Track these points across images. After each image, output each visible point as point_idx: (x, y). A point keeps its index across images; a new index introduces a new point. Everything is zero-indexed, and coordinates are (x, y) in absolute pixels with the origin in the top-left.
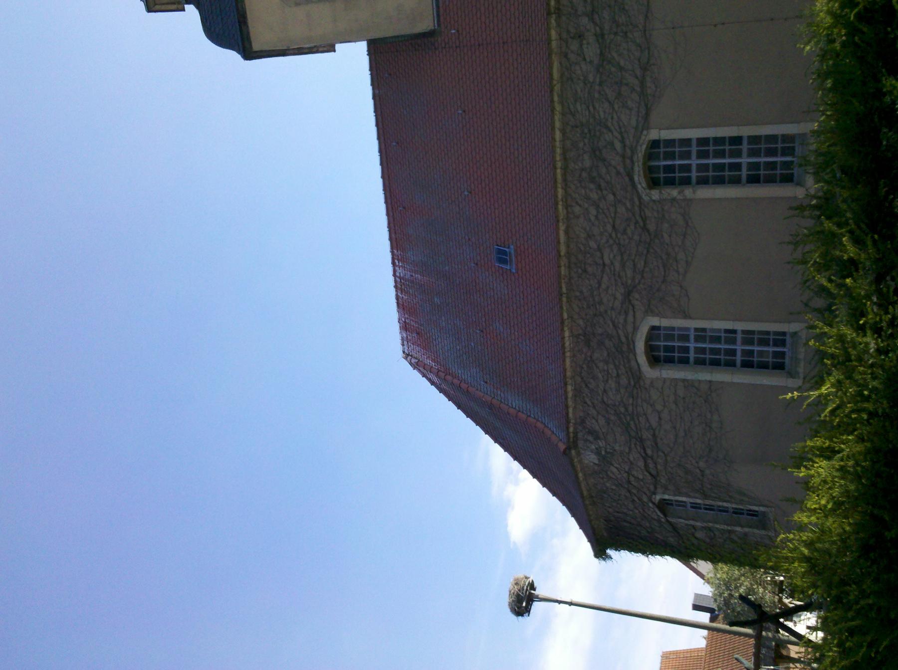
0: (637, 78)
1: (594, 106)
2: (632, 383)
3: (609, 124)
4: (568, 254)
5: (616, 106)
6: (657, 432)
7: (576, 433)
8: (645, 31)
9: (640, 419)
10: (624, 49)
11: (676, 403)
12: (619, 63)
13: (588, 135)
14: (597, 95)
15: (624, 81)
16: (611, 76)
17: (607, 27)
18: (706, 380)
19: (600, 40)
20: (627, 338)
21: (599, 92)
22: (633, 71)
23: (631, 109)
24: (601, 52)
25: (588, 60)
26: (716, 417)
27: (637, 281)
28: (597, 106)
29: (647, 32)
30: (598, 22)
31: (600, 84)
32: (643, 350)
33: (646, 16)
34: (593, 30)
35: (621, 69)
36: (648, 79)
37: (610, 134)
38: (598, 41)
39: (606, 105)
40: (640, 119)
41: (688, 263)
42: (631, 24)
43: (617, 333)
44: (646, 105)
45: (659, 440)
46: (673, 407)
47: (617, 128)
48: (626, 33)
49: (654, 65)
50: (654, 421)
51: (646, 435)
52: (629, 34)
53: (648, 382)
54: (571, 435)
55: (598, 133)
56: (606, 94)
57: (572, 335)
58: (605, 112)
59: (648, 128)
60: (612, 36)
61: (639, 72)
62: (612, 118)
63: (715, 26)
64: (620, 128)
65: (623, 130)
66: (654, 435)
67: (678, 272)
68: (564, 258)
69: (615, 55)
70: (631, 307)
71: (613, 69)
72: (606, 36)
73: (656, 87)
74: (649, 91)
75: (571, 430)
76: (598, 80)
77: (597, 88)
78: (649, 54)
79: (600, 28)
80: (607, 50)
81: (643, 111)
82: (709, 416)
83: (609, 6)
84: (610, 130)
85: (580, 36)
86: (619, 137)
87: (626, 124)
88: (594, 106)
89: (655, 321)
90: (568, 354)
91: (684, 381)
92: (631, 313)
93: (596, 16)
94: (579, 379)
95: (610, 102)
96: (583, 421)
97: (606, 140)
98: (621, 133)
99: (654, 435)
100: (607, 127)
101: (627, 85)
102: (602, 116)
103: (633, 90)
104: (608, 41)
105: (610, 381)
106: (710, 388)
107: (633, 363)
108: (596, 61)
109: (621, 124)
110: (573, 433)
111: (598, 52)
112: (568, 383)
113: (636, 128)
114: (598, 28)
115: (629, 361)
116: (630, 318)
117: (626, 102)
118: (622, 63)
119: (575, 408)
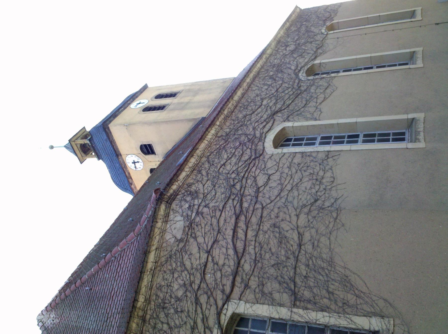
2: (253, 157)
4: (239, 102)
6: (261, 189)
7: (176, 194)
9: (249, 181)
11: (289, 168)
18: (324, 151)
20: (261, 134)
26: (329, 174)
27: (283, 109)
32: (272, 139)
41: (325, 99)
43: (255, 133)
45: (260, 195)
46: (286, 171)
50: (261, 180)
51: (249, 191)
53: (267, 157)
54: (171, 191)
57: (216, 135)
66: (258, 191)
67: (317, 102)
68: (234, 102)
70: (272, 120)
75: (174, 187)
82: (321, 173)
89: (289, 124)
90: (206, 142)
91: (302, 153)
92: (272, 122)
94: (204, 159)
96: (190, 185)
99: (258, 191)
105: (232, 159)
106: (327, 156)
107: (260, 147)
110: (174, 191)
112: (194, 157)
115: (257, 145)
116: (270, 124)
119: (188, 176)
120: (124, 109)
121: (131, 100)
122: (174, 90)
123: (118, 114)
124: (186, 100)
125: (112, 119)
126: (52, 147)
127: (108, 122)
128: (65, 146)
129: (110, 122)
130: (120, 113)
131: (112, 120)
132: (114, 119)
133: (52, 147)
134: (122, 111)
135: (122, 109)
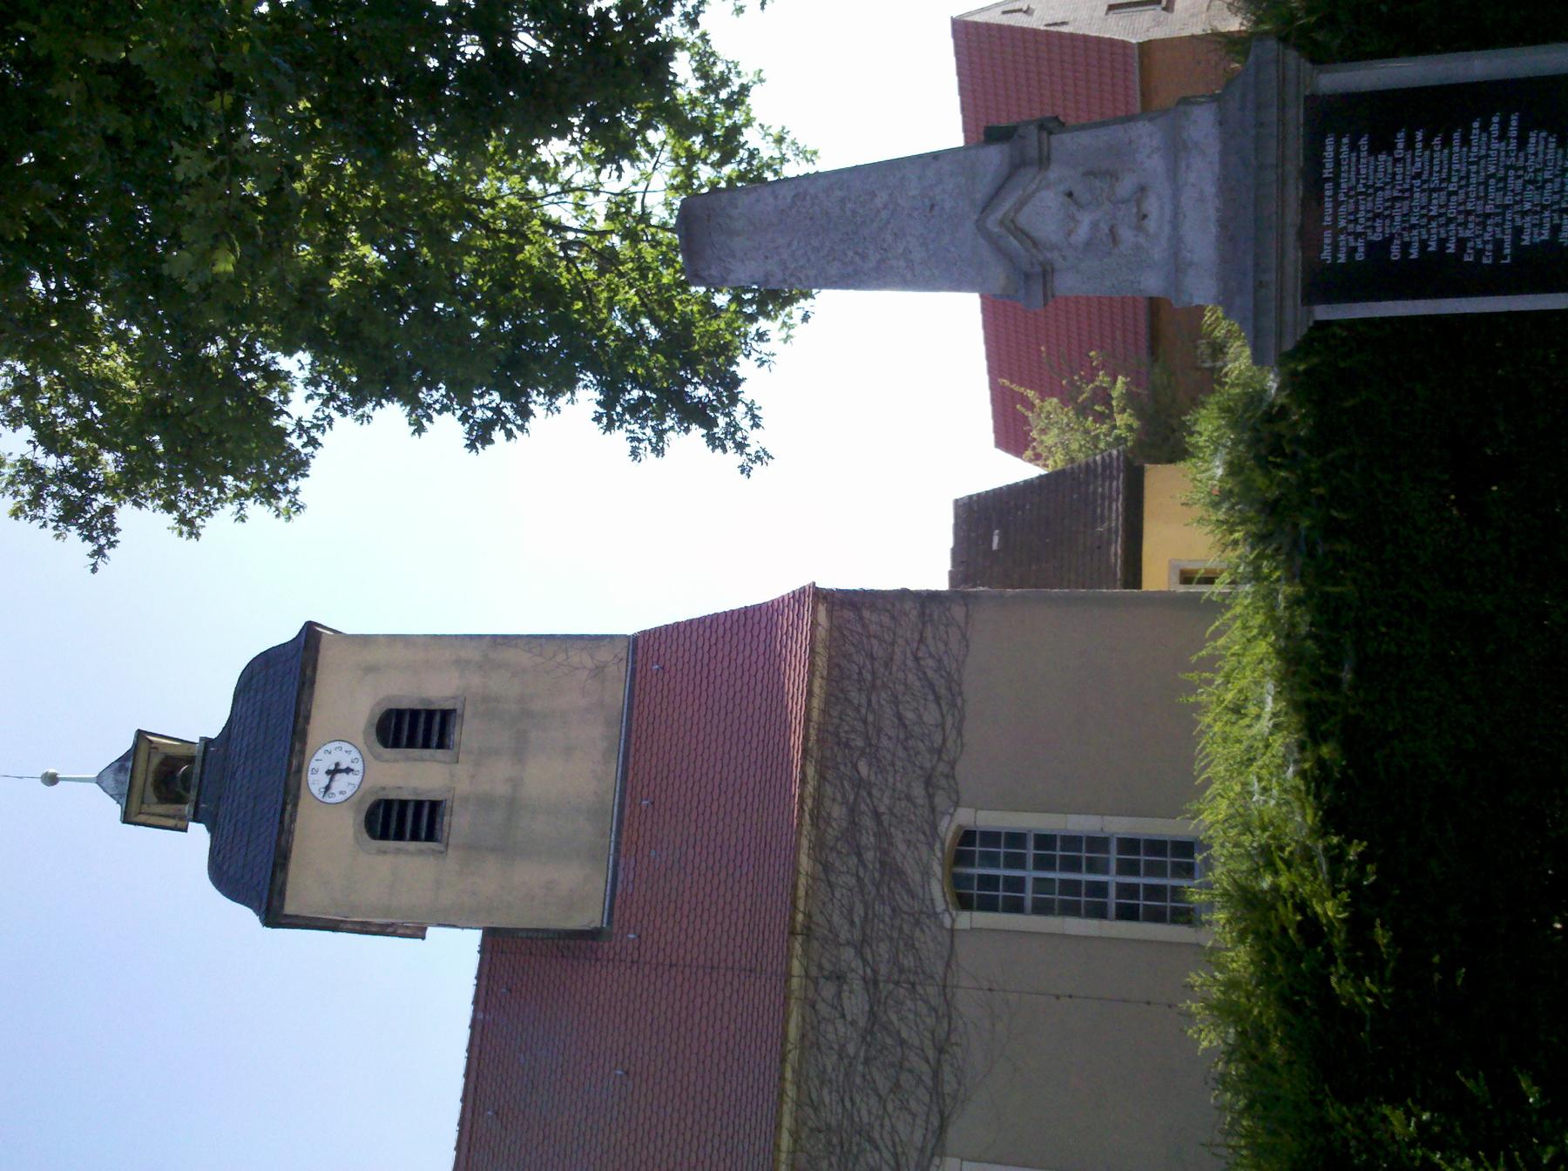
0: (927, 1061)
1: (851, 1099)
3: (876, 1136)
5: (890, 1107)
8: (945, 986)
10: (909, 1010)
12: (899, 1033)
13: (838, 1150)
14: (858, 1080)
15: (907, 1064)
16: (886, 1053)
17: (883, 969)
19: (872, 990)
21: (864, 1076)
22: (922, 1050)
23: (914, 1116)
24: (871, 1007)
25: (849, 1018)
28: (858, 1100)
29: (948, 990)
30: (869, 957)
31: (867, 1062)
33: (948, 965)
34: (861, 972)
35: (902, 1042)
36: (947, 1068)
37: (877, 1156)
38: (868, 990)
39: (873, 1101)
40: (929, 1135)
42: (924, 973)
44: (941, 1113)
47: (890, 1144)
48: (913, 985)
49: (957, 1044)
52: (918, 988)
55: (855, 1149)
56: (874, 1081)
58: (870, 1112)
59: (943, 1155)
60: (891, 986)
61: (931, 1054)
62: (882, 1126)
63: (1058, 997)
64: (894, 1146)
65: (899, 1150)
69: (894, 1018)
71: (889, 1041)
72: (881, 985)
73: (959, 1083)
74: (947, 1089)
76: (862, 1054)
77: (860, 1068)
78: (950, 1024)
79: (874, 971)
80: (882, 1007)
81: (935, 1121)
83: (891, 939)
84: (877, 1148)
85: (839, 978)
86: (892, 1163)
87: (904, 1138)
88: (851, 1099)
93: (867, 951)
95: (879, 1096)
97: (867, 1164)
98: (895, 1155)
100: (871, 1140)
101: (911, 1071)
102: (866, 1120)
103: (920, 1080)
104: (884, 993)
108: (862, 1022)
109: (897, 1139)
111: (867, 1008)
113: (922, 1151)
114: (868, 971)
117: (907, 1100)
118: (904, 1035)
120: (295, 805)
121: (298, 747)
122: (435, 689)
123: (287, 841)
124: (496, 777)
125: (279, 876)
126: (51, 780)
127: (275, 903)
128: (99, 780)
129: (282, 894)
130: (291, 833)
131: (284, 884)
132: (286, 873)
133: (51, 780)
134: (293, 820)
135: (289, 807)
